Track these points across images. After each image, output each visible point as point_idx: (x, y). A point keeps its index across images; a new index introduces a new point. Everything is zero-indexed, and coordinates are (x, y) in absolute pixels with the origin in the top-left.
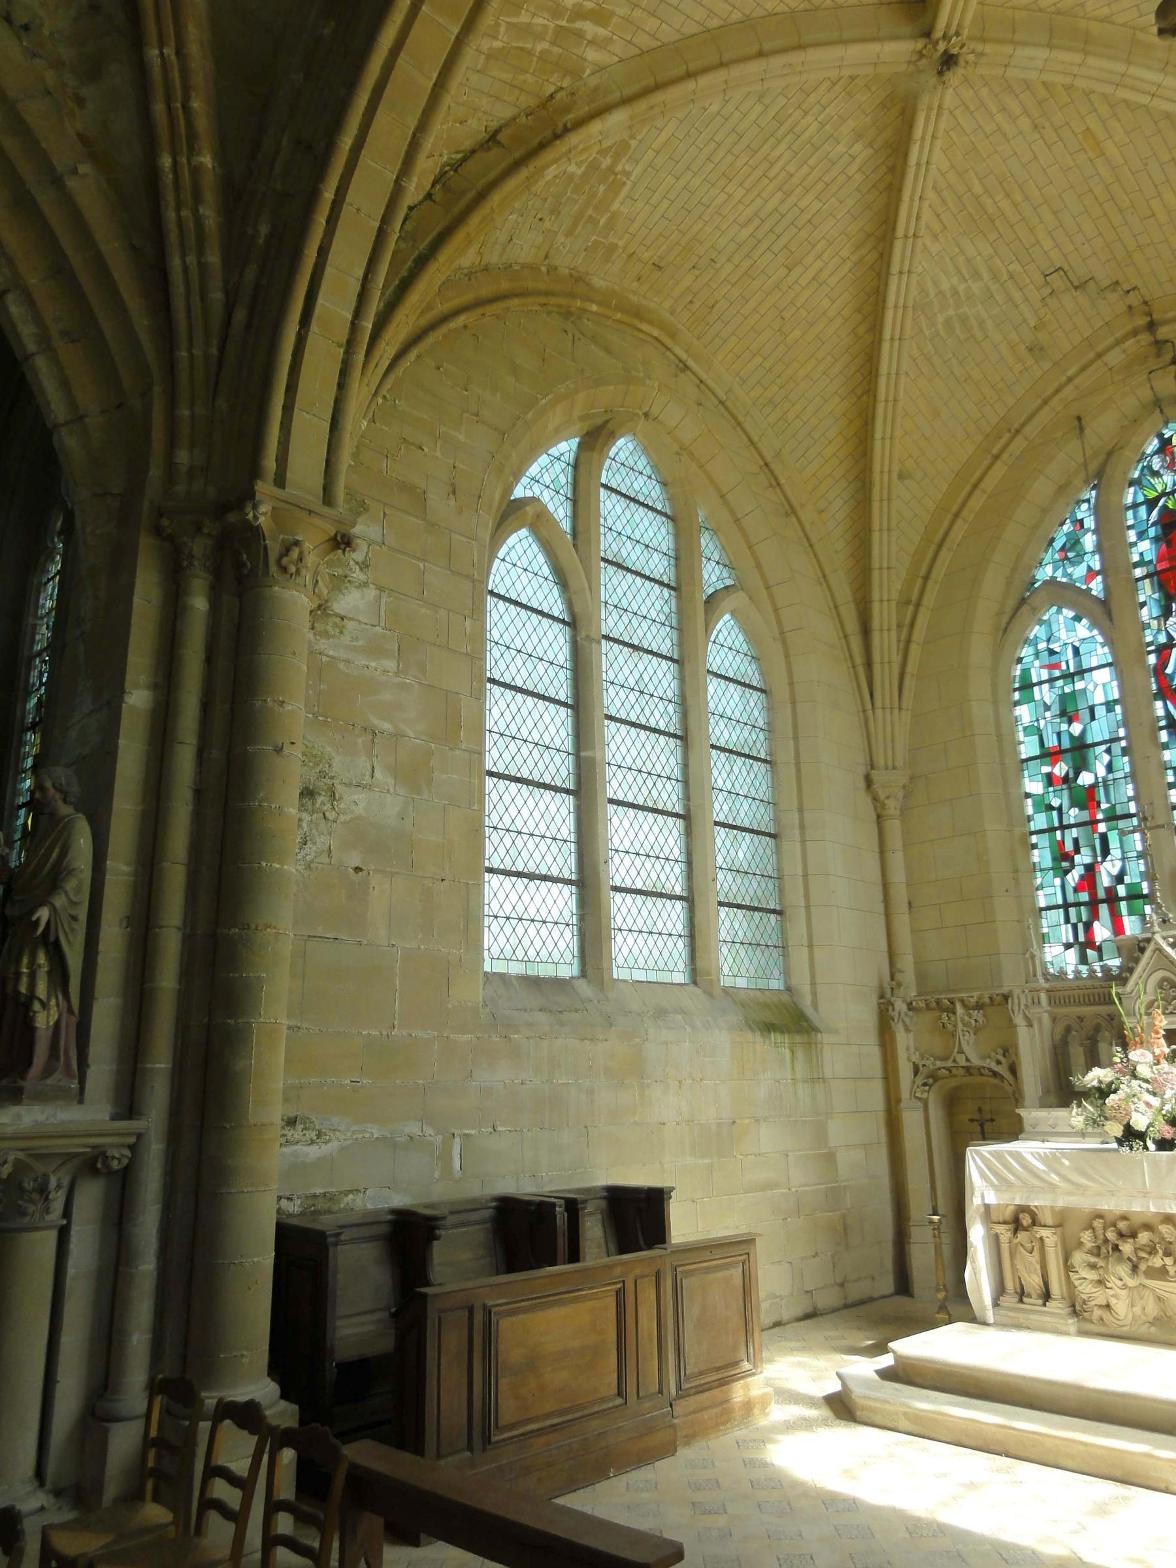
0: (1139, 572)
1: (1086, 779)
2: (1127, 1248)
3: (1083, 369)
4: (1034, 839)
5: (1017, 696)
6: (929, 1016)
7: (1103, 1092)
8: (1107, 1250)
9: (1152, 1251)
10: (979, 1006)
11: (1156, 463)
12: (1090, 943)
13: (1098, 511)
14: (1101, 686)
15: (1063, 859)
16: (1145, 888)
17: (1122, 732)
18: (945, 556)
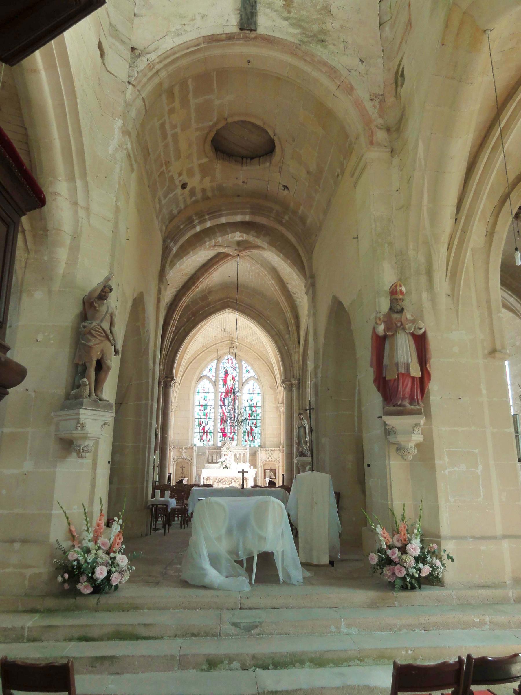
1: (206, 411)
3: (220, 342)
5: (197, 393)
6: (177, 450)
7: (222, 462)
11: (227, 361)
12: (202, 439)
14: (211, 396)
15: (200, 424)
16: (212, 431)
17: (213, 405)
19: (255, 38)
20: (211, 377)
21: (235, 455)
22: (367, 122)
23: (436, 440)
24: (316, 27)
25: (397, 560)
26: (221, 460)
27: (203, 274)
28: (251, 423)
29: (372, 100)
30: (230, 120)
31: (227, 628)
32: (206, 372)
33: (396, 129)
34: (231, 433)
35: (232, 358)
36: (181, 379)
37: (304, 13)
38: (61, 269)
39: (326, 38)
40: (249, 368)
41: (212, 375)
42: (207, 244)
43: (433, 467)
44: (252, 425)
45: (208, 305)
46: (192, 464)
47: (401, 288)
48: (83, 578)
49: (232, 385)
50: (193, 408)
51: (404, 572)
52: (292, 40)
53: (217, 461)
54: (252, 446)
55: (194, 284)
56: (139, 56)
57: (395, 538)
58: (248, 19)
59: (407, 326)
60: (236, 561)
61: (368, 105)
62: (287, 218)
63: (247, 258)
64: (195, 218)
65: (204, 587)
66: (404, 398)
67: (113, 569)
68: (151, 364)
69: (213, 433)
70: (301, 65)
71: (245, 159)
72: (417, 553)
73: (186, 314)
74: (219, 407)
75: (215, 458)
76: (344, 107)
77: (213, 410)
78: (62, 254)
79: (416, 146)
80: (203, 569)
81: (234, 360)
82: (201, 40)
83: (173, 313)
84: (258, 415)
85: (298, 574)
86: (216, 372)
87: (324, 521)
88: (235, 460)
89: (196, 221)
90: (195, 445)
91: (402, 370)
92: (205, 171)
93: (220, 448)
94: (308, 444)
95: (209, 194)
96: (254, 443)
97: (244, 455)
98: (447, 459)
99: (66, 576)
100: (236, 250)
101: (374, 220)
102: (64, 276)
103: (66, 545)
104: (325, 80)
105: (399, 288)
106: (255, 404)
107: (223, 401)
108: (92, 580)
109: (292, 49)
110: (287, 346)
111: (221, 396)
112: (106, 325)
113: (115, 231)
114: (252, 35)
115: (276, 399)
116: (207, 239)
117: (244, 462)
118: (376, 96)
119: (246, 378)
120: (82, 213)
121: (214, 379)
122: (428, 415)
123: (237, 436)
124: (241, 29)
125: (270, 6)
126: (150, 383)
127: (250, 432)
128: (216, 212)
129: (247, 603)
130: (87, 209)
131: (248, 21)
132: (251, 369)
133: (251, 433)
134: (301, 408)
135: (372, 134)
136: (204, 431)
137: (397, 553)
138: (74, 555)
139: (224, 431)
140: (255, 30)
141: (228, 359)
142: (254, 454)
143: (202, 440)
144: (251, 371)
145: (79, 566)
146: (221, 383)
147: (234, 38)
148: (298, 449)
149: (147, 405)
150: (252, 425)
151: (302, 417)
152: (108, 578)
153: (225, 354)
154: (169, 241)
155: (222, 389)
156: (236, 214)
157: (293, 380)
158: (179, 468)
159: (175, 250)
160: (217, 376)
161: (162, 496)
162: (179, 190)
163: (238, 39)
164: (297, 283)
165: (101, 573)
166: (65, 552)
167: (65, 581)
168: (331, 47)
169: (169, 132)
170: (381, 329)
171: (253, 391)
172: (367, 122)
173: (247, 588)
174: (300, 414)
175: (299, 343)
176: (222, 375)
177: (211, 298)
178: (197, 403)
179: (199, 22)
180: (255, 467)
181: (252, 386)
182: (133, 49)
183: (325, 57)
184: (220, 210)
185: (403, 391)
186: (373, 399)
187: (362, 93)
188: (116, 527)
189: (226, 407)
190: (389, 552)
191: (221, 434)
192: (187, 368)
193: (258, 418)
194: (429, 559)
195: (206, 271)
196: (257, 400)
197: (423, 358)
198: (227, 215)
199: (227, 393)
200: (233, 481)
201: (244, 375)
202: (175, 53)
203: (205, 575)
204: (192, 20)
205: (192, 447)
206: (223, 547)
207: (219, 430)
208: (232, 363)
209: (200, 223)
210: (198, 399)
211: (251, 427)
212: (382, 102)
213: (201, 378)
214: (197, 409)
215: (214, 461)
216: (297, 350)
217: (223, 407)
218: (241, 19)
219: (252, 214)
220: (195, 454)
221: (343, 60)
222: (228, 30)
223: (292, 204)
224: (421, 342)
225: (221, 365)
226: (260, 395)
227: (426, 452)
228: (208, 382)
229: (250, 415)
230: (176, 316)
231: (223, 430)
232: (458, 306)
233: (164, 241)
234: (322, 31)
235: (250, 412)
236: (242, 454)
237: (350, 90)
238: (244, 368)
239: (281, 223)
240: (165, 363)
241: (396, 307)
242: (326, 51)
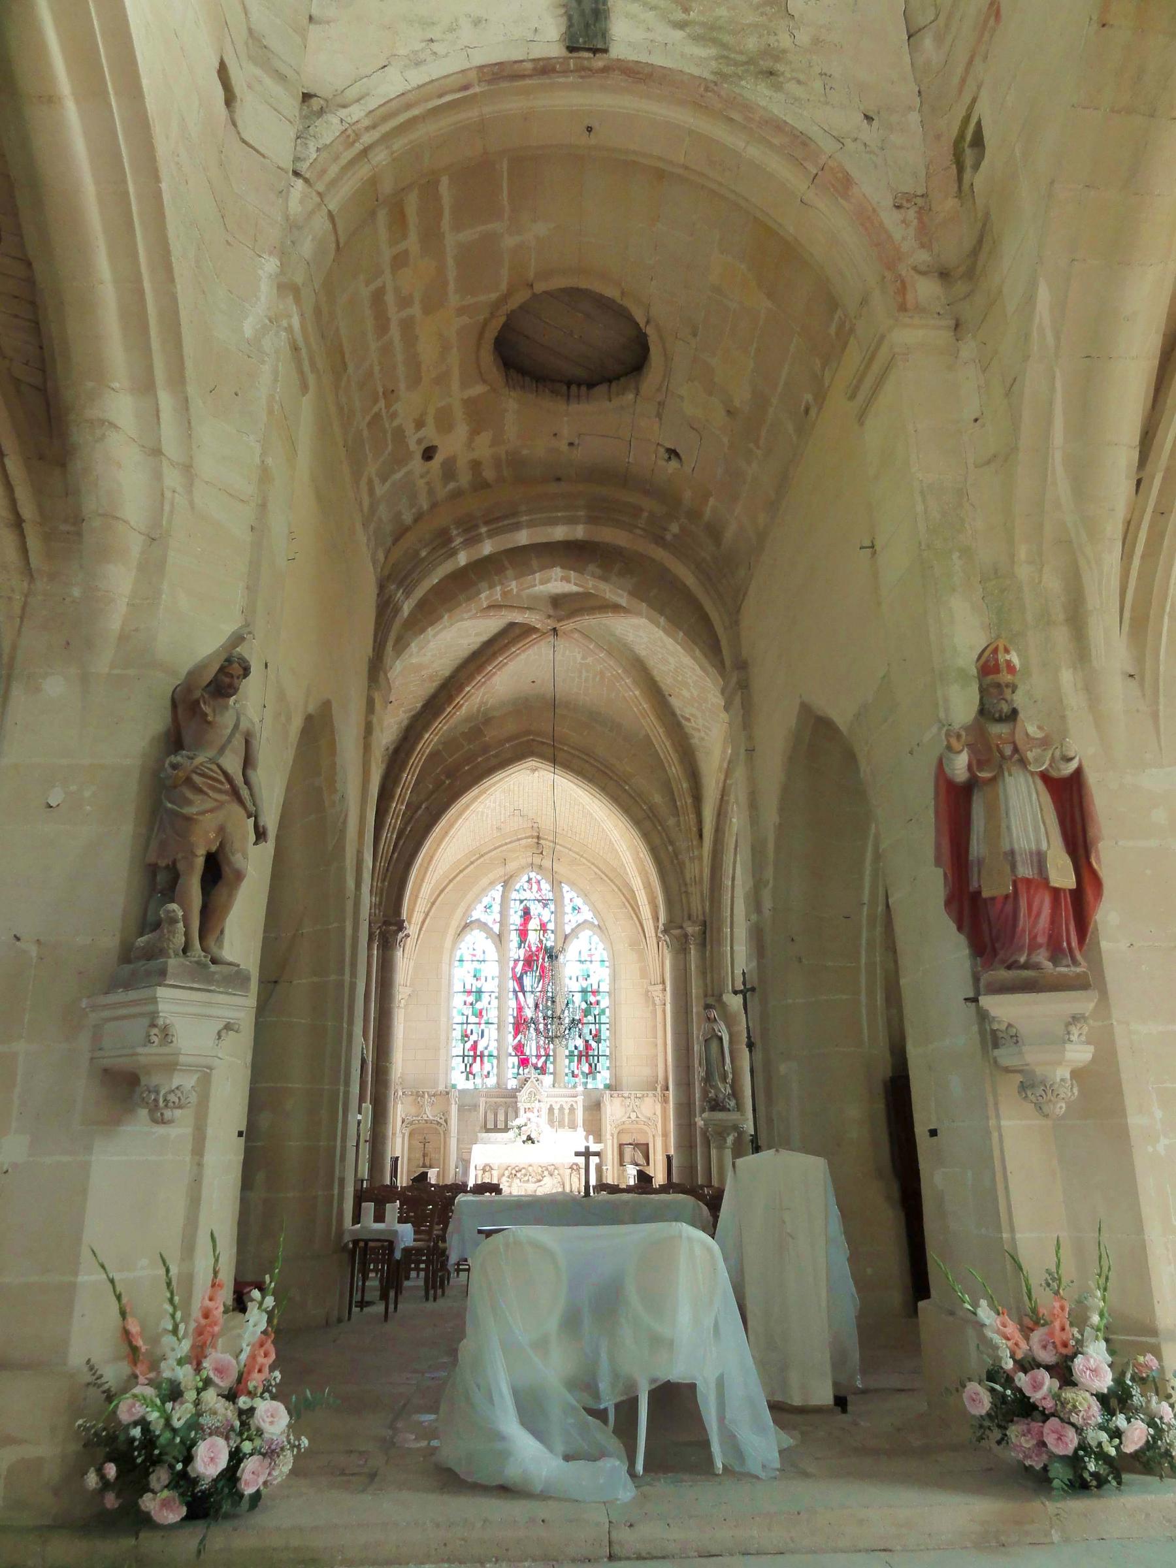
0: (513, 927)
1: (479, 1006)
2: (519, 1175)
4: (455, 1026)
5: (457, 963)
6: (411, 1098)
7: (519, 1128)
8: (513, 1176)
9: (525, 1175)
10: (434, 1095)
11: (526, 886)
12: (471, 1073)
13: (503, 897)
14: (491, 969)
15: (465, 1036)
16: (495, 1053)
18: (442, 895)
19: (605, 70)
20: (490, 924)
21: (551, 1109)
22: (889, 259)
24: (752, 44)
25: (1049, 1404)
26: (517, 1122)
27: (470, 678)
28: (586, 1030)
30: (540, 287)
32: (478, 913)
34: (538, 1057)
35: (539, 877)
36: (420, 930)
38: (115, 620)
39: (779, 67)
40: (579, 902)
41: (492, 919)
42: (483, 596)
44: (589, 1038)
45: (485, 749)
46: (446, 1132)
47: (1008, 657)
48: (160, 1477)
49: (541, 941)
50: (449, 999)
51: (1072, 1441)
52: (696, 72)
53: (506, 1125)
54: (590, 1086)
55: (450, 699)
56: (321, 112)
57: (1037, 1336)
58: (587, 25)
59: (1030, 755)
60: (591, 1412)
62: (675, 528)
63: (576, 635)
64: (455, 532)
65: (505, 1490)
66: (1033, 947)
67: (247, 1447)
68: (351, 883)
69: (498, 1058)
70: (719, 132)
71: (574, 388)
72: (1105, 1382)
73: (433, 772)
74: (511, 995)
75: (501, 1117)
76: (828, 231)
77: (495, 1003)
78: (120, 581)
79: (1030, 300)
80: (502, 1437)
81: (543, 882)
82: (473, 75)
83: (402, 769)
84: (603, 1012)
85: (763, 1443)
86: (501, 913)
88: (551, 1122)
89: (459, 540)
90: (454, 1086)
91: (1025, 871)
92: (480, 416)
93: (513, 1094)
94: (729, 1080)
95: (489, 474)
96: (594, 1079)
98: (1159, 1114)
99: (111, 1470)
100: (549, 617)
101: (922, 493)
102: (123, 638)
103: (113, 1373)
104: (776, 165)
105: (1002, 657)
106: (595, 987)
107: (520, 981)
108: (184, 1481)
109: (698, 94)
110: (672, 843)
111: (513, 969)
112: (232, 763)
113: (258, 529)
114: (599, 62)
115: (644, 973)
116: (484, 585)
117: (573, 1126)
118: (910, 197)
119: (574, 925)
120: (172, 478)
121: (496, 928)
123: (554, 1063)
124: (571, 49)
126: (349, 931)
127: (585, 1054)
128: (506, 517)
129: (626, 1538)
130: (188, 469)
131: (586, 31)
132: (585, 903)
133: (587, 1056)
134: (710, 992)
135: (903, 289)
136: (476, 1054)
137: (1049, 1383)
138: (137, 1408)
139: (522, 1053)
140: (606, 51)
142: (594, 1107)
143: (469, 1073)
144: (585, 909)
145: (149, 1440)
146: (514, 937)
147: (554, 70)
148: (705, 1093)
149: (340, 985)
150: (589, 1038)
151: (714, 1013)
152: (231, 1474)
153: (521, 869)
154: (393, 587)
155: (516, 952)
156: (553, 522)
157: (690, 927)
158: (415, 1142)
159: (407, 608)
160: (503, 922)
161: (379, 1217)
162: (417, 464)
163: (566, 72)
164: (695, 693)
165: (210, 1460)
166: (110, 1397)
167: (106, 1485)
168: (792, 87)
169: (394, 315)
170: (960, 765)
171: (591, 956)
172: (889, 259)
173: (626, 1492)
174: (708, 1007)
175: (701, 836)
176: (516, 919)
177: (491, 734)
178: (458, 987)
179: (467, 34)
182: (306, 97)
184: (514, 514)
185: (1024, 929)
186: (939, 954)
188: (256, 1320)
189: (528, 994)
190: (1022, 1380)
191: (516, 1060)
192: (433, 904)
193: (604, 1019)
194: (1137, 1399)
195: (480, 669)
196: (600, 976)
197: (1077, 836)
198: (531, 524)
199: (529, 962)
200: (546, 1173)
202: (409, 106)
203: (504, 1455)
204: (451, 30)
205: (447, 1093)
206: (553, 1370)
207: (511, 1050)
208: (539, 889)
210: (461, 976)
211: (587, 1041)
212: (924, 212)
213: (466, 926)
214: (458, 1000)
215: (501, 1125)
216: (696, 853)
217: (520, 995)
219: (592, 520)
220: (454, 1109)
222: (538, 52)
223: (687, 495)
224: (1069, 796)
225: (514, 895)
226: (607, 964)
227: (1101, 1091)
230: (409, 777)
231: (519, 1048)
232: (1157, 703)
233: (382, 587)
234: (769, 52)
235: (584, 1006)
236: (567, 1107)
237: (844, 184)
238: (567, 901)
239: (659, 540)
240: (382, 890)
242: (780, 96)
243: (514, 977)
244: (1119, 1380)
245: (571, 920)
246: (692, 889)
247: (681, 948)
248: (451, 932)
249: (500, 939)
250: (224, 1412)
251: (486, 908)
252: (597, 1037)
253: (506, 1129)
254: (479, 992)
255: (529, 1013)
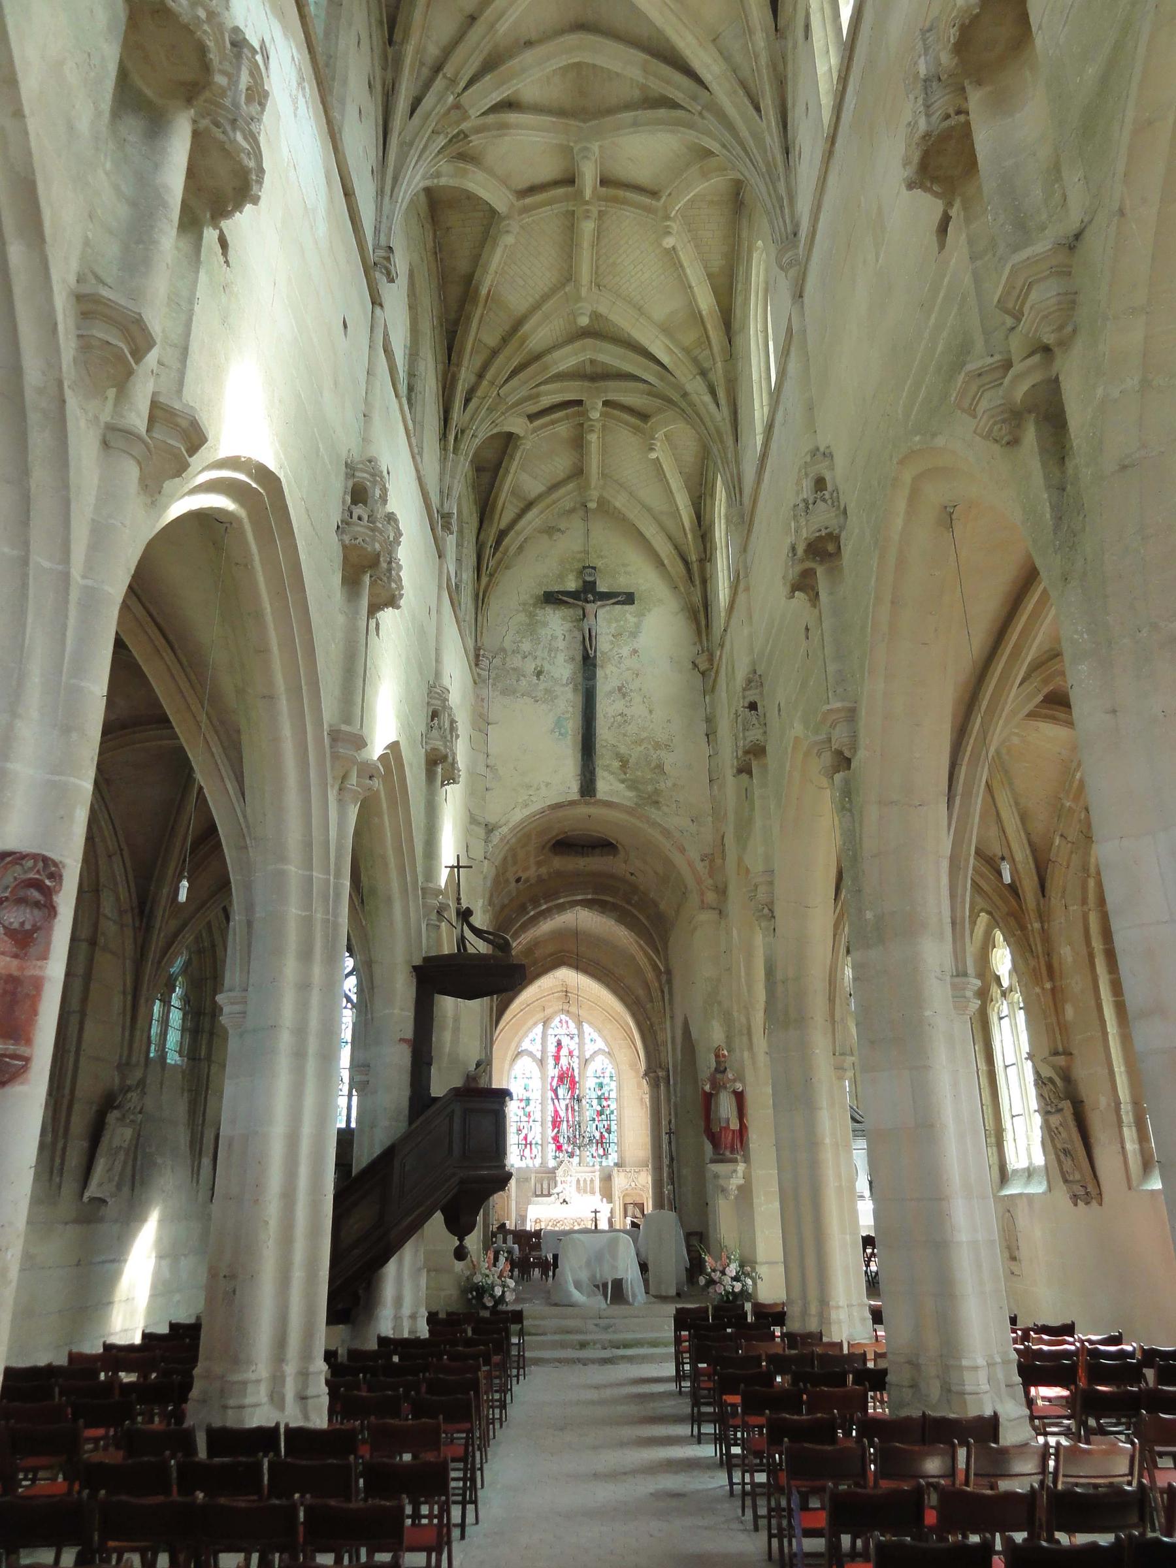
1: (527, 1110)
11: (559, 1025)
14: (536, 1084)
21: (578, 1181)
22: (699, 882)
23: (754, 1181)
24: (650, 788)
28: (600, 1125)
29: (702, 860)
31: (592, 1327)
32: (526, 1045)
33: (722, 891)
37: (639, 773)
40: (595, 1035)
41: (536, 1049)
43: (751, 1204)
44: (603, 1130)
52: (628, 803)
54: (604, 1164)
56: (492, 831)
61: (700, 867)
66: (726, 1148)
74: (550, 1101)
75: (545, 1186)
76: (678, 859)
78: (447, 1036)
84: (612, 1112)
87: (671, 1260)
88: (578, 1189)
91: (723, 1124)
93: (553, 1171)
97: (592, 1181)
107: (555, 1091)
108: (492, 1296)
110: (649, 1019)
115: (639, 1086)
117: (593, 1193)
121: (539, 1055)
122: (747, 1160)
125: (607, 768)
131: (588, 787)
133: (602, 1143)
135: (702, 894)
136: (527, 1143)
138: (478, 1279)
141: (561, 1021)
142: (607, 1179)
143: (522, 1157)
146: (551, 1061)
150: (603, 1130)
153: (556, 1013)
155: (553, 1072)
156: (574, 895)
160: (544, 1051)
162: (514, 884)
165: (498, 1291)
167: (473, 1298)
172: (699, 882)
173: (604, 1306)
176: (552, 1049)
180: (610, 1201)
181: (600, 1064)
183: (658, 820)
187: (694, 854)
191: (554, 1147)
193: (613, 1117)
194: (742, 1278)
199: (561, 1079)
201: (586, 1047)
206: (584, 1276)
207: (551, 1140)
209: (533, 909)
213: (519, 1053)
218: (582, 786)
221: (676, 821)
224: (740, 1097)
225: (550, 1031)
227: (745, 1192)
228: (530, 1059)
229: (600, 1113)
231: (556, 1139)
235: (599, 1108)
236: (588, 1180)
237: (682, 850)
238: (586, 1035)
239: (629, 903)
241: (721, 1069)
243: (552, 1089)
244: (737, 1273)
245: (589, 1049)
246: (662, 1048)
247: (655, 1084)
248: (509, 1058)
249: (541, 1062)
250: (499, 1281)
251: (532, 1041)
252: (609, 1131)
253: (549, 1195)
254: (528, 1100)
255: (562, 1114)
